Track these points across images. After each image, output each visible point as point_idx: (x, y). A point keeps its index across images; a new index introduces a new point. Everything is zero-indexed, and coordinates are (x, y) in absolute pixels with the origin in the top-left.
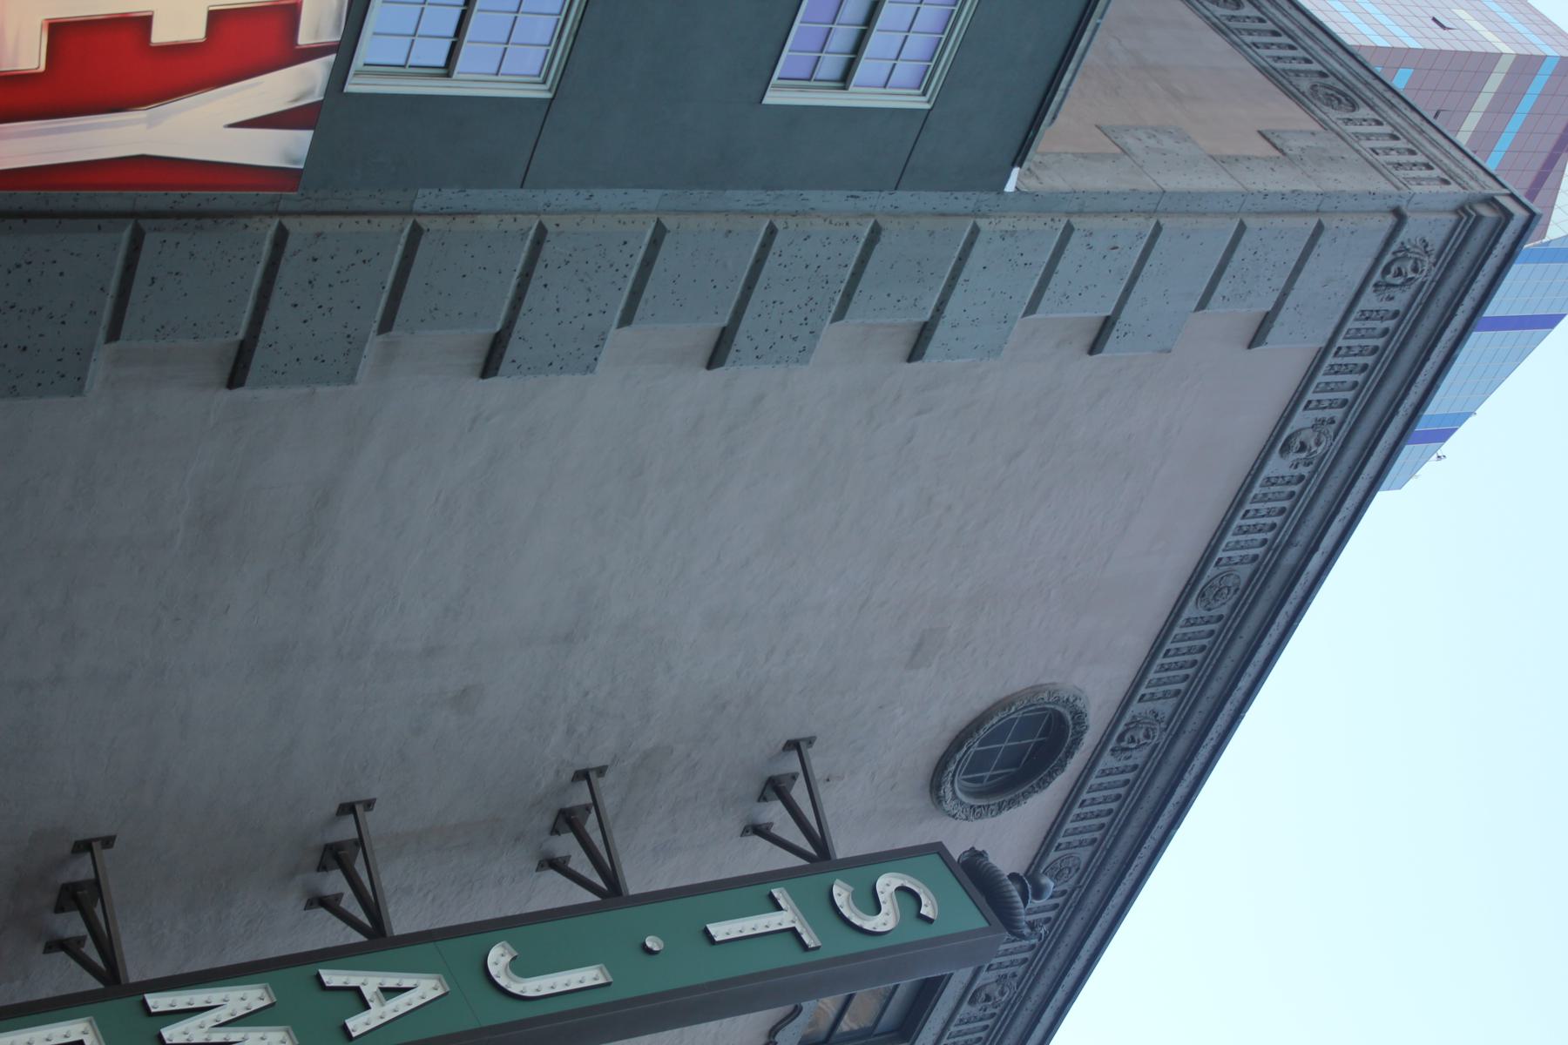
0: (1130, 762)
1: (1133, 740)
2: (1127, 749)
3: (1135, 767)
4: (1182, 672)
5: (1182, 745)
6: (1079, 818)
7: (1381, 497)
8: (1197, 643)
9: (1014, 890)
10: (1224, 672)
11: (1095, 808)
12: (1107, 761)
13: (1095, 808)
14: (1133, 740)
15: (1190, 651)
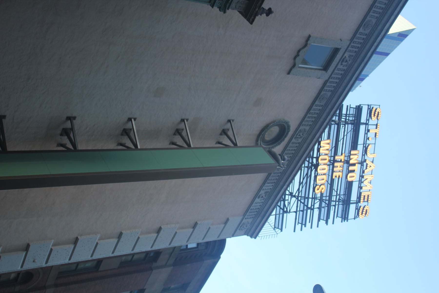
0: (298, 142)
1: (299, 135)
2: (298, 138)
3: (299, 143)
4: (278, 175)
5: (310, 138)
6: (250, 212)
7: (350, 93)
8: (294, 149)
9: (279, 157)
10: (321, 120)
11: (290, 152)
12: (293, 140)
13: (290, 152)
14: (299, 135)
15: (292, 150)
